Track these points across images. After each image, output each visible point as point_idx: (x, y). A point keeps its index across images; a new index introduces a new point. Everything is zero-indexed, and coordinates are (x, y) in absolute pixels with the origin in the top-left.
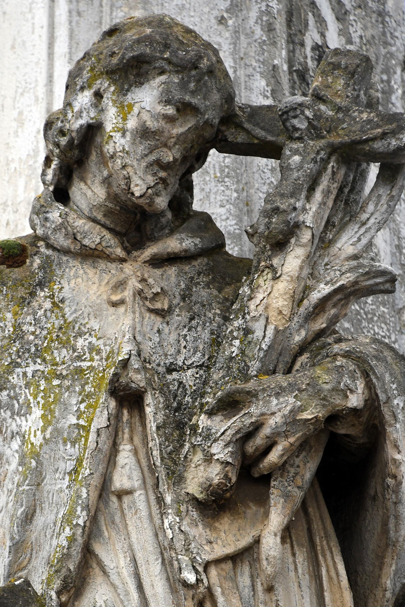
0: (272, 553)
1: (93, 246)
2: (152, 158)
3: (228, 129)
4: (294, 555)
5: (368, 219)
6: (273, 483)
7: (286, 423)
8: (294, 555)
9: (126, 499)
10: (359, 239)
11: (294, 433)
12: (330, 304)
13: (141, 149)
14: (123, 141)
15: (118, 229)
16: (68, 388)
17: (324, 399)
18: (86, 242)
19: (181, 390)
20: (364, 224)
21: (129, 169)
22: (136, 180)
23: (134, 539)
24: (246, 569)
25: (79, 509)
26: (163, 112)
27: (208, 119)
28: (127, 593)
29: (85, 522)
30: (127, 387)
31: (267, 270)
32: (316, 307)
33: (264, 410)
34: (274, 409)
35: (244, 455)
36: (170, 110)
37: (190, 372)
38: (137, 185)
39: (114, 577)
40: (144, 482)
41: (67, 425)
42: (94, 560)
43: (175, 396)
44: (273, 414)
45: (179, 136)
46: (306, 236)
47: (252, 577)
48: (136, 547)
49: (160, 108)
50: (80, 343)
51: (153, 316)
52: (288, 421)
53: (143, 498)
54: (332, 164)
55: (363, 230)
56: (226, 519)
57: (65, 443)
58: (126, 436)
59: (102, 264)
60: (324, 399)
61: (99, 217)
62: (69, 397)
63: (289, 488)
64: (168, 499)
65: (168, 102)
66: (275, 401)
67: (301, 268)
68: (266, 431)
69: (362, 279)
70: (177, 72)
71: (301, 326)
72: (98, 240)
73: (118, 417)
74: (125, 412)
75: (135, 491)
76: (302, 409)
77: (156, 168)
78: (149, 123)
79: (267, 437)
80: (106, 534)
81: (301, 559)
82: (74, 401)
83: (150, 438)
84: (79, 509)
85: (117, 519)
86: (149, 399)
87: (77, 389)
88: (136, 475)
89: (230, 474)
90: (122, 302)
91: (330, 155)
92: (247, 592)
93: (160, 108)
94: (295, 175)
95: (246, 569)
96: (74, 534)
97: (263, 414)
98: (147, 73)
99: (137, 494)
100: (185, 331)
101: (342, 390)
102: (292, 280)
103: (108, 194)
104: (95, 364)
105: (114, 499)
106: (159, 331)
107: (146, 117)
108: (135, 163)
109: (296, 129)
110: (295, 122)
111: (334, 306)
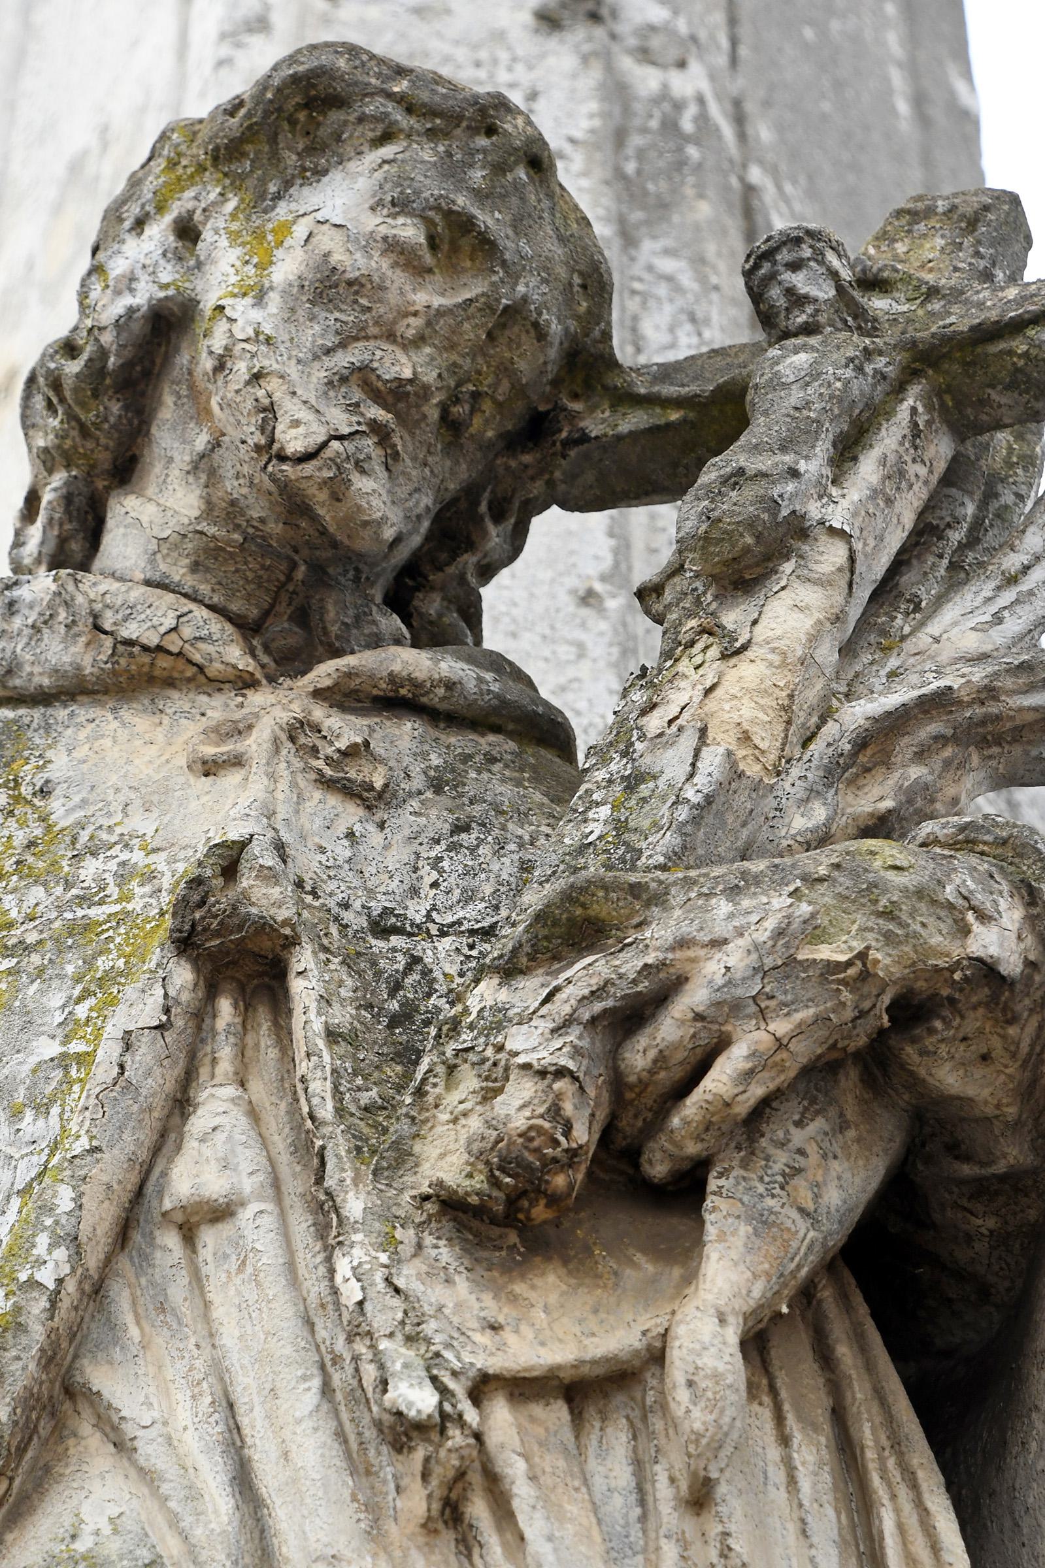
0: (709, 1361)
1: (153, 640)
2: (343, 359)
3: (592, 409)
4: (784, 1440)
5: (1026, 569)
6: (713, 1184)
7: (759, 970)
8: (784, 1440)
9: (210, 1238)
10: (998, 619)
11: (788, 1008)
12: (905, 746)
13: (313, 334)
14: (256, 315)
15: (235, 607)
16: (41, 971)
17: (888, 914)
18: (131, 631)
19: (415, 976)
20: (1012, 580)
21: (273, 384)
22: (289, 408)
23: (229, 1337)
24: (619, 1439)
25: (43, 1240)
26: (383, 230)
27: (525, 299)
28: (193, 1495)
29: (60, 1281)
30: (234, 920)
31: (705, 639)
32: (862, 743)
33: (688, 929)
34: (721, 929)
35: (618, 1084)
36: (410, 231)
37: (447, 943)
38: (296, 423)
39: (150, 1451)
40: (276, 1184)
41: (26, 1069)
42: (87, 1412)
43: (395, 988)
44: (718, 943)
45: (435, 316)
46: (831, 556)
47: (638, 1465)
48: (237, 1359)
49: (372, 222)
50: (90, 868)
51: (334, 801)
52: (769, 962)
53: (268, 1221)
54: (910, 402)
55: (1008, 596)
56: (551, 1278)
57: (16, 1114)
58: (225, 1066)
59: (178, 701)
60: (888, 914)
61: (178, 572)
62: (42, 992)
63: (770, 1202)
64: (354, 1205)
65: (400, 206)
66: (723, 907)
67: (814, 639)
68: (695, 997)
69: (1009, 683)
70: (432, 134)
71: (812, 793)
72: (170, 622)
73: (201, 1015)
74: (225, 1007)
75: (243, 1204)
76: (814, 932)
77: (357, 395)
78: (335, 258)
79: (699, 1017)
80: (134, 1332)
81: (811, 1458)
82: (56, 999)
83: (300, 1054)
84: (43, 1240)
85: (178, 1291)
86: (304, 958)
87: (70, 969)
88: (248, 1159)
89: (568, 1108)
90: (237, 762)
91: (910, 374)
92: (620, 1506)
93: (372, 222)
94: (796, 396)
95: (619, 1439)
96: (18, 1310)
97: (682, 943)
98: (338, 139)
99: (246, 1215)
100: (438, 850)
101: (951, 906)
102: (784, 664)
103: (209, 506)
104: (136, 905)
105: (171, 1240)
106: (350, 835)
107: (328, 241)
108: (293, 370)
109: (797, 300)
110: (798, 281)
111: (921, 755)
